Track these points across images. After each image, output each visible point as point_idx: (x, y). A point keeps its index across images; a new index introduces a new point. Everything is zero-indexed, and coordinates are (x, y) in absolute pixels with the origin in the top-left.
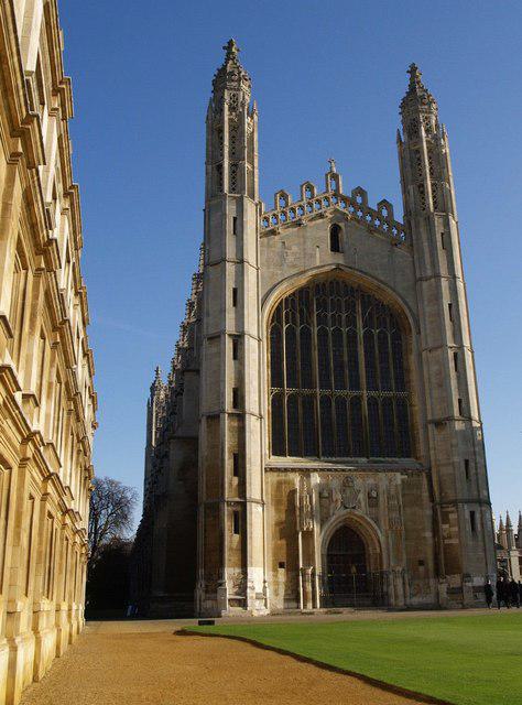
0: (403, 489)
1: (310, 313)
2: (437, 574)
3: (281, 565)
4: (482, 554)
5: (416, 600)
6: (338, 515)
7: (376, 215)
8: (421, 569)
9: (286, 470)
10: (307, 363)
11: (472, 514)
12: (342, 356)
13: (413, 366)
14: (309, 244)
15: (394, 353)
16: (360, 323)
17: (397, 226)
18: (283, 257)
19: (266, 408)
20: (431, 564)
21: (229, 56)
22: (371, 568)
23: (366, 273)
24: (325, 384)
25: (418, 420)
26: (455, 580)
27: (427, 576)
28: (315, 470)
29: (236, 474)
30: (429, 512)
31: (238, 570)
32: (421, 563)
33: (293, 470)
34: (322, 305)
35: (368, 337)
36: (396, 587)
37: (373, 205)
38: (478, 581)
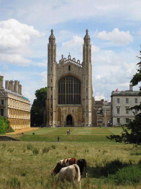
1: (65, 81)
2: (82, 122)
3: (59, 120)
6: (67, 113)
7: (77, 63)
10: (64, 89)
11: (87, 114)
13: (82, 90)
15: (79, 87)
17: (80, 64)
19: (57, 97)
20: (81, 121)
21: (52, 34)
22: (73, 121)
24: (67, 93)
25: (82, 99)
26: (84, 123)
32: (80, 120)
34: (67, 79)
35: (75, 84)
36: (76, 124)
37: (76, 61)
38: (87, 123)
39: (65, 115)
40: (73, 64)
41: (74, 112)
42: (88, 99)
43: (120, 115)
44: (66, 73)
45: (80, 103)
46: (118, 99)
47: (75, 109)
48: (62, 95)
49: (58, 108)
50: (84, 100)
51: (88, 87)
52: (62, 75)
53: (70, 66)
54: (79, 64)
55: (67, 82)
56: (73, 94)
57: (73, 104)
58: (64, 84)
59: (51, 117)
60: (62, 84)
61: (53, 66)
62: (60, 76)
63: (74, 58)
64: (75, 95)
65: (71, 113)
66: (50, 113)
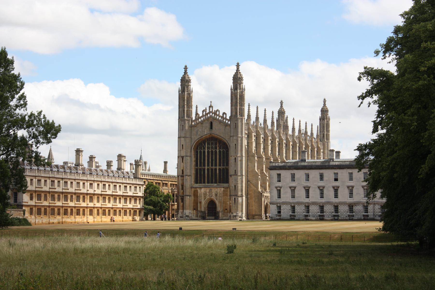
0: (223, 192)
3: (195, 209)
4: (236, 208)
5: (224, 218)
6: (208, 197)
8: (226, 211)
9: (196, 188)
10: (204, 160)
11: (235, 199)
12: (213, 157)
14: (204, 128)
16: (218, 148)
17: (228, 119)
18: (197, 133)
19: (193, 172)
20: (228, 210)
23: (218, 135)
24: (208, 165)
25: (229, 175)
27: (227, 213)
28: (202, 188)
29: (182, 189)
30: (229, 197)
31: (182, 210)
32: (226, 209)
33: (198, 188)
34: (208, 144)
35: (220, 152)
37: (221, 115)
38: (235, 214)
39: (205, 199)
40: (216, 119)
41: (217, 196)
42: (237, 175)
43: (282, 201)
44: (206, 134)
45: (227, 182)
46: (279, 175)
47: (218, 192)
48: (200, 169)
49: (193, 190)
50: (231, 176)
51: (236, 156)
52: (200, 137)
53: (211, 123)
54: (226, 119)
55: (208, 148)
56: (218, 167)
57: (216, 182)
58: (204, 152)
59: (182, 203)
60: (201, 152)
61: (185, 123)
62: (196, 139)
63: (217, 110)
64: (219, 169)
65: (214, 198)
66: (179, 197)
